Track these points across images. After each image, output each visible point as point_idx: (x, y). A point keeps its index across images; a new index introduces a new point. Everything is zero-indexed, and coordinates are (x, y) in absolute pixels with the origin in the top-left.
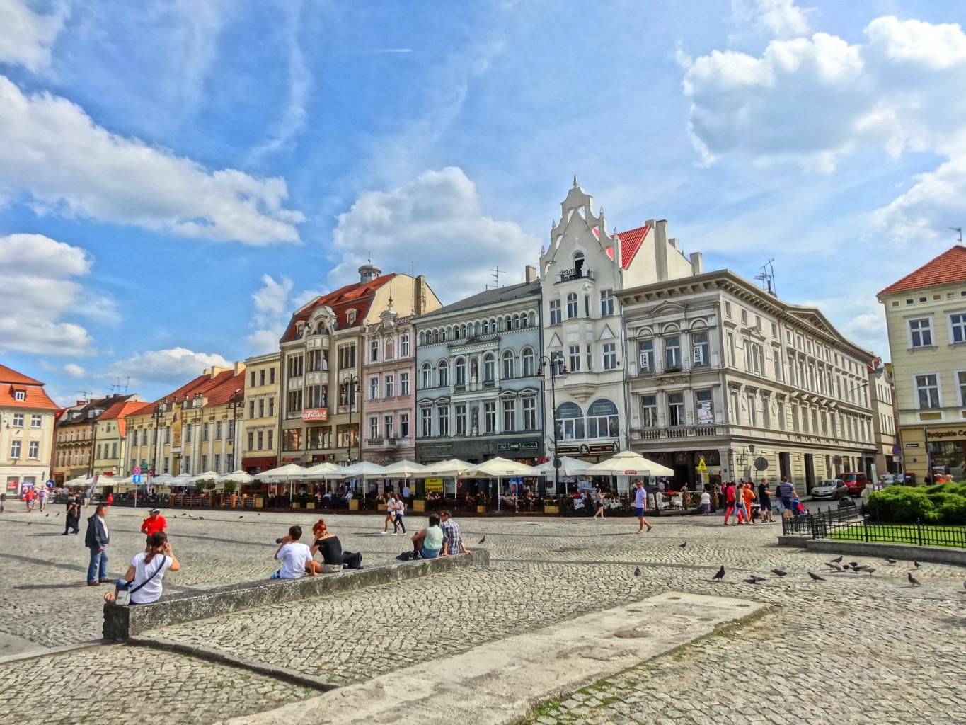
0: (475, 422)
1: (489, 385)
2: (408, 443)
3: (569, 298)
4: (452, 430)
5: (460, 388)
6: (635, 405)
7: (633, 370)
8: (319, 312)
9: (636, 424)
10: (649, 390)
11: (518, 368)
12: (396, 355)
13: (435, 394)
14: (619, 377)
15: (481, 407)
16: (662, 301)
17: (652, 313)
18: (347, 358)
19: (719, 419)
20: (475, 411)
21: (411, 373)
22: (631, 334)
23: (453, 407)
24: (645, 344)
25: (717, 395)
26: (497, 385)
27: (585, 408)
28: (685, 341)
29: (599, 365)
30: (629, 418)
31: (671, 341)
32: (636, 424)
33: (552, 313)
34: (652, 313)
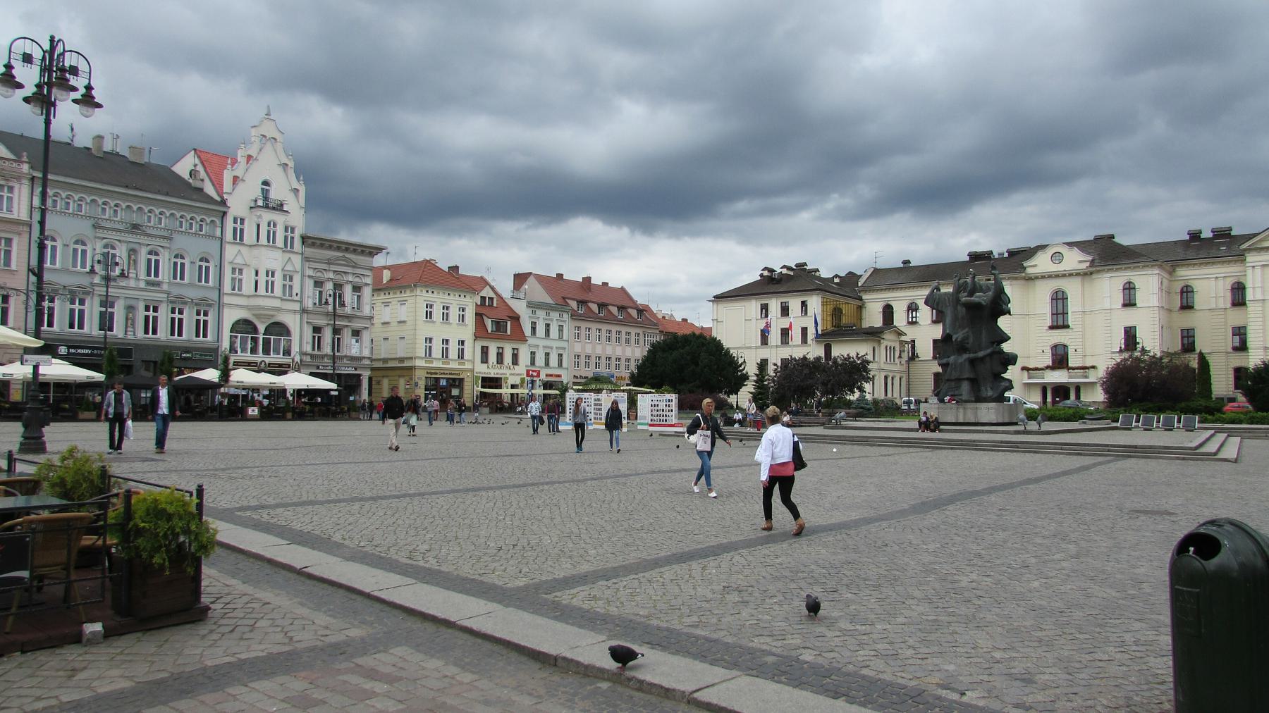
3: (269, 225)
7: (309, 304)
9: (308, 349)
10: (320, 321)
14: (297, 307)
15: (141, 306)
16: (340, 254)
17: (329, 262)
19: (366, 353)
22: (311, 273)
23: (97, 301)
26: (165, 287)
27: (262, 328)
30: (300, 339)
33: (235, 229)
34: (329, 262)
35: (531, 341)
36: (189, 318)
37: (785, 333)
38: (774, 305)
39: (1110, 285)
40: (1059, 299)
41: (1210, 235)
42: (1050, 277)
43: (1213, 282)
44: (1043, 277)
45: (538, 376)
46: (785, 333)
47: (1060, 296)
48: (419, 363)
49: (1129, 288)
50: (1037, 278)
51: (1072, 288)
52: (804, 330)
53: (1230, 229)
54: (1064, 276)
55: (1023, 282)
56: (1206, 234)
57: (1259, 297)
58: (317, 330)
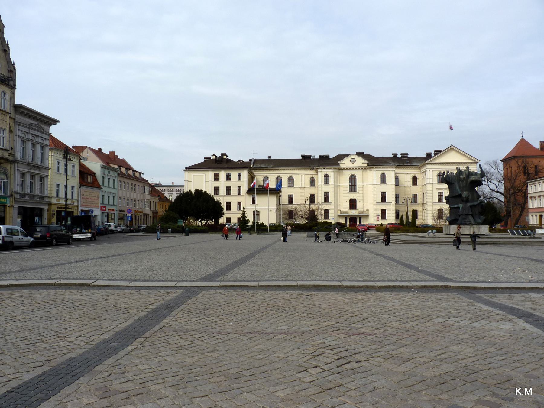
35: (104, 189)
37: (228, 189)
38: (222, 174)
39: (374, 174)
40: (353, 179)
41: (400, 156)
42: (350, 169)
43: (406, 175)
44: (347, 169)
45: (105, 210)
46: (228, 189)
47: (353, 178)
48: (54, 201)
49: (383, 176)
50: (344, 169)
51: (358, 174)
52: (239, 189)
53: (407, 154)
54: (356, 169)
55: (337, 170)
56: (399, 156)
57: (431, 182)
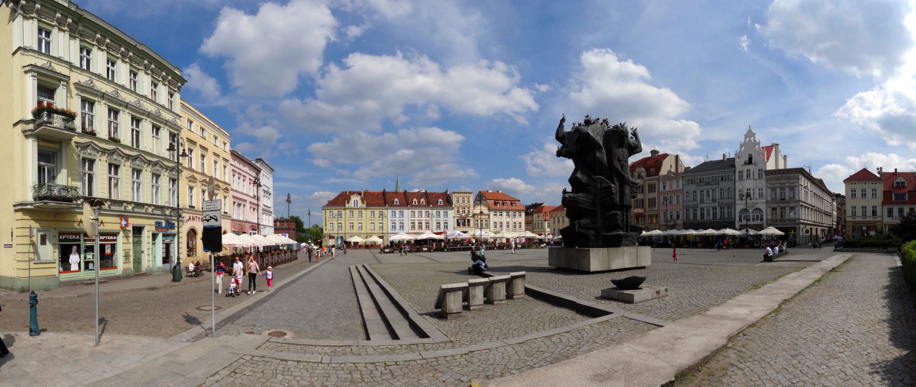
0: (709, 215)
1: (714, 200)
2: (680, 222)
4: (699, 218)
5: (702, 201)
6: (770, 210)
7: (769, 199)
8: (638, 170)
9: (770, 217)
10: (775, 206)
11: (726, 196)
12: (674, 187)
13: (691, 204)
14: (764, 201)
18: (652, 188)
20: (708, 210)
21: (681, 195)
24: (773, 190)
25: (797, 209)
28: (787, 189)
29: (757, 196)
30: (767, 214)
31: (783, 189)
32: (770, 217)
36: (726, 210)
58: (774, 209)
